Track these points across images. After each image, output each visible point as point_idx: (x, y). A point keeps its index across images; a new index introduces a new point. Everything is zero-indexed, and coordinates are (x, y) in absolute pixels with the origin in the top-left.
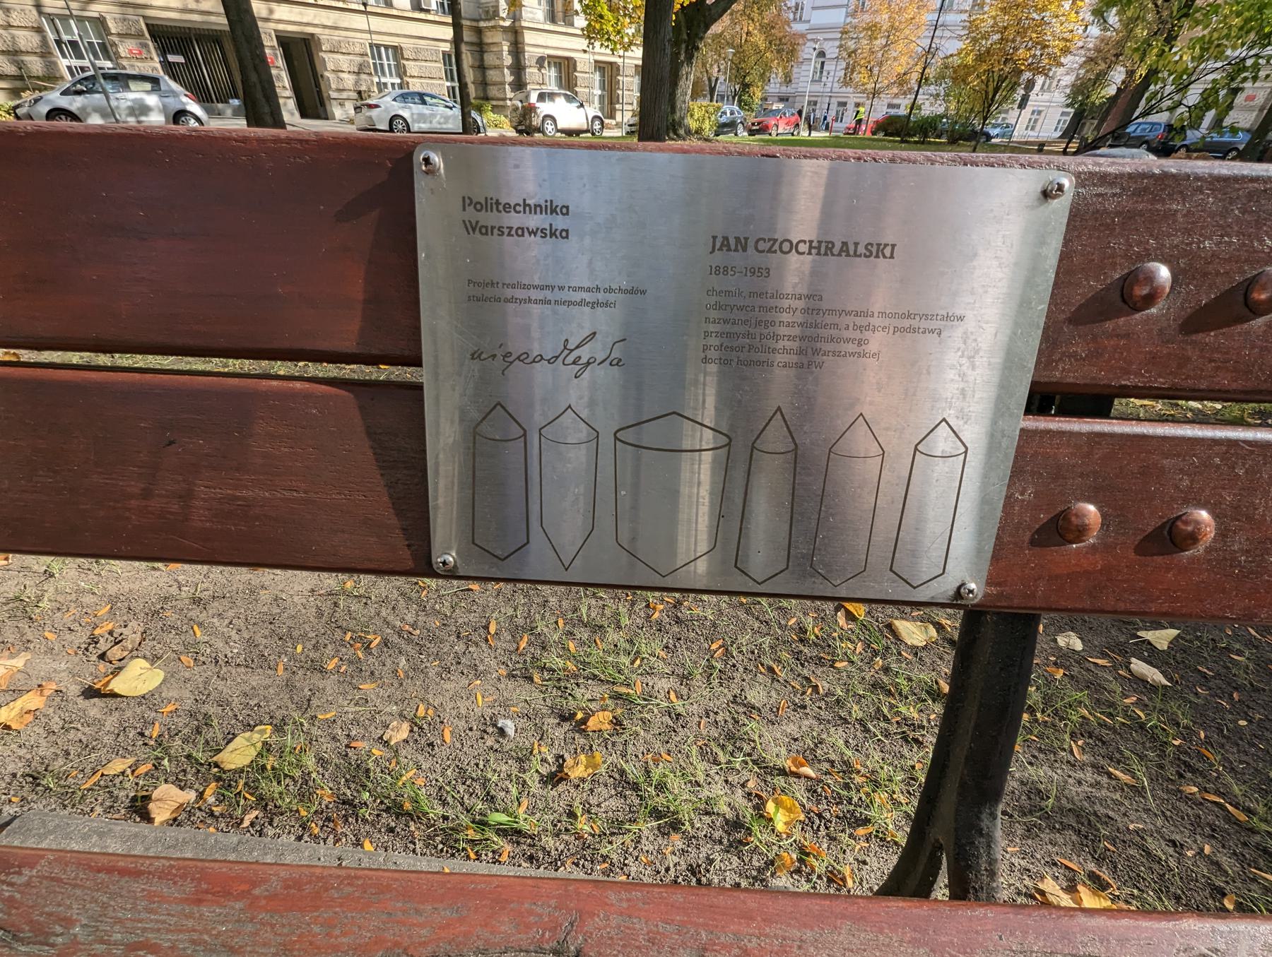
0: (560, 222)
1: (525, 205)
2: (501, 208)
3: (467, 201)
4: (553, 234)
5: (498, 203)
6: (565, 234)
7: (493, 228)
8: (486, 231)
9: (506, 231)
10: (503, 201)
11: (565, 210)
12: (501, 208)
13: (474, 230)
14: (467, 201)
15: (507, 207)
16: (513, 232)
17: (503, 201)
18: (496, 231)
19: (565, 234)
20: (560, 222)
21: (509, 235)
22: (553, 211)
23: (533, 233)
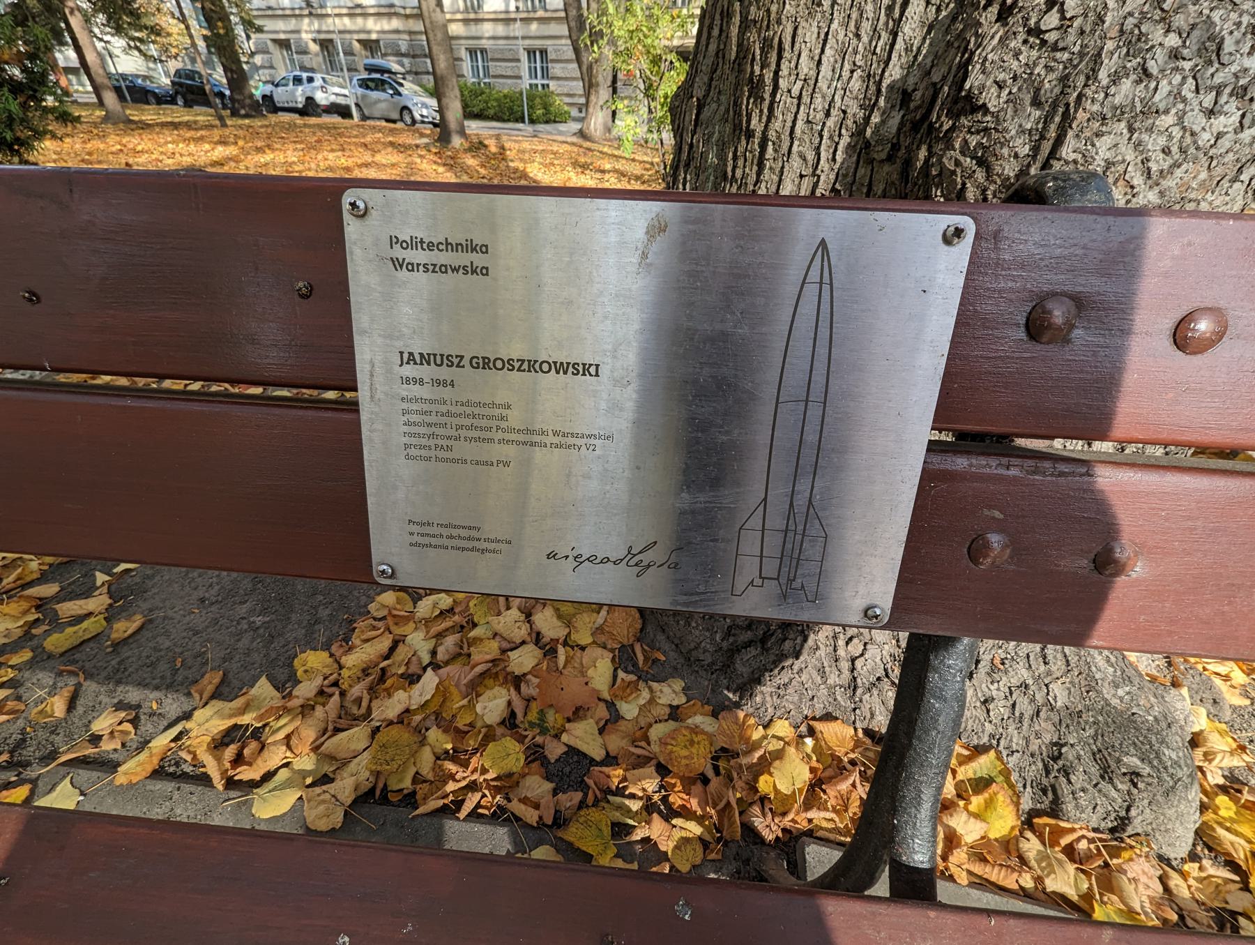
0: (478, 260)
1: (447, 244)
2: (425, 246)
3: (394, 240)
4: (474, 272)
5: (422, 242)
6: (485, 271)
7: (418, 265)
8: (412, 267)
9: (431, 268)
10: (426, 240)
11: (484, 249)
12: (425, 246)
13: (401, 266)
14: (394, 240)
15: (431, 246)
16: (437, 269)
17: (426, 240)
18: (421, 268)
19: (485, 271)
20: (478, 260)
21: (433, 271)
22: (474, 249)
23: (455, 270)
